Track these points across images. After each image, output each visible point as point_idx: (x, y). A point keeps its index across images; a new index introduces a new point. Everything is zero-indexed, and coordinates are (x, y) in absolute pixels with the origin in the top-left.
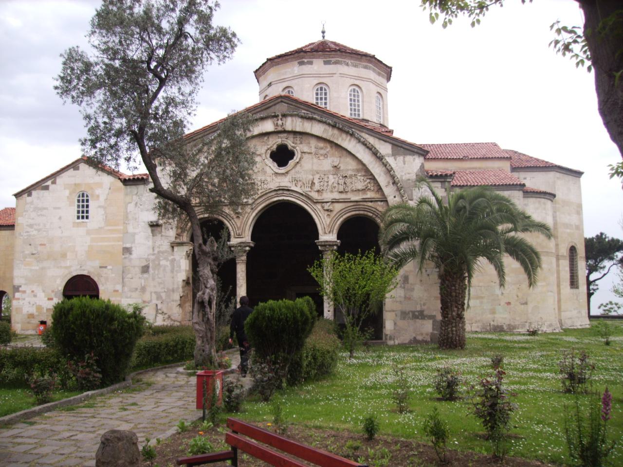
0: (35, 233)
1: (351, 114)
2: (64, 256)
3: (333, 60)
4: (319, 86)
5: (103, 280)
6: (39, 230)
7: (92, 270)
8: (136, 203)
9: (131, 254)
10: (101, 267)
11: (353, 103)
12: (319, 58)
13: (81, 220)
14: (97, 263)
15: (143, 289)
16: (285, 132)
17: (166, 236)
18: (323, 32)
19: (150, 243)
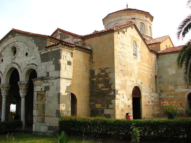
0: (121, 57)
6: (123, 56)
18: (127, 6)
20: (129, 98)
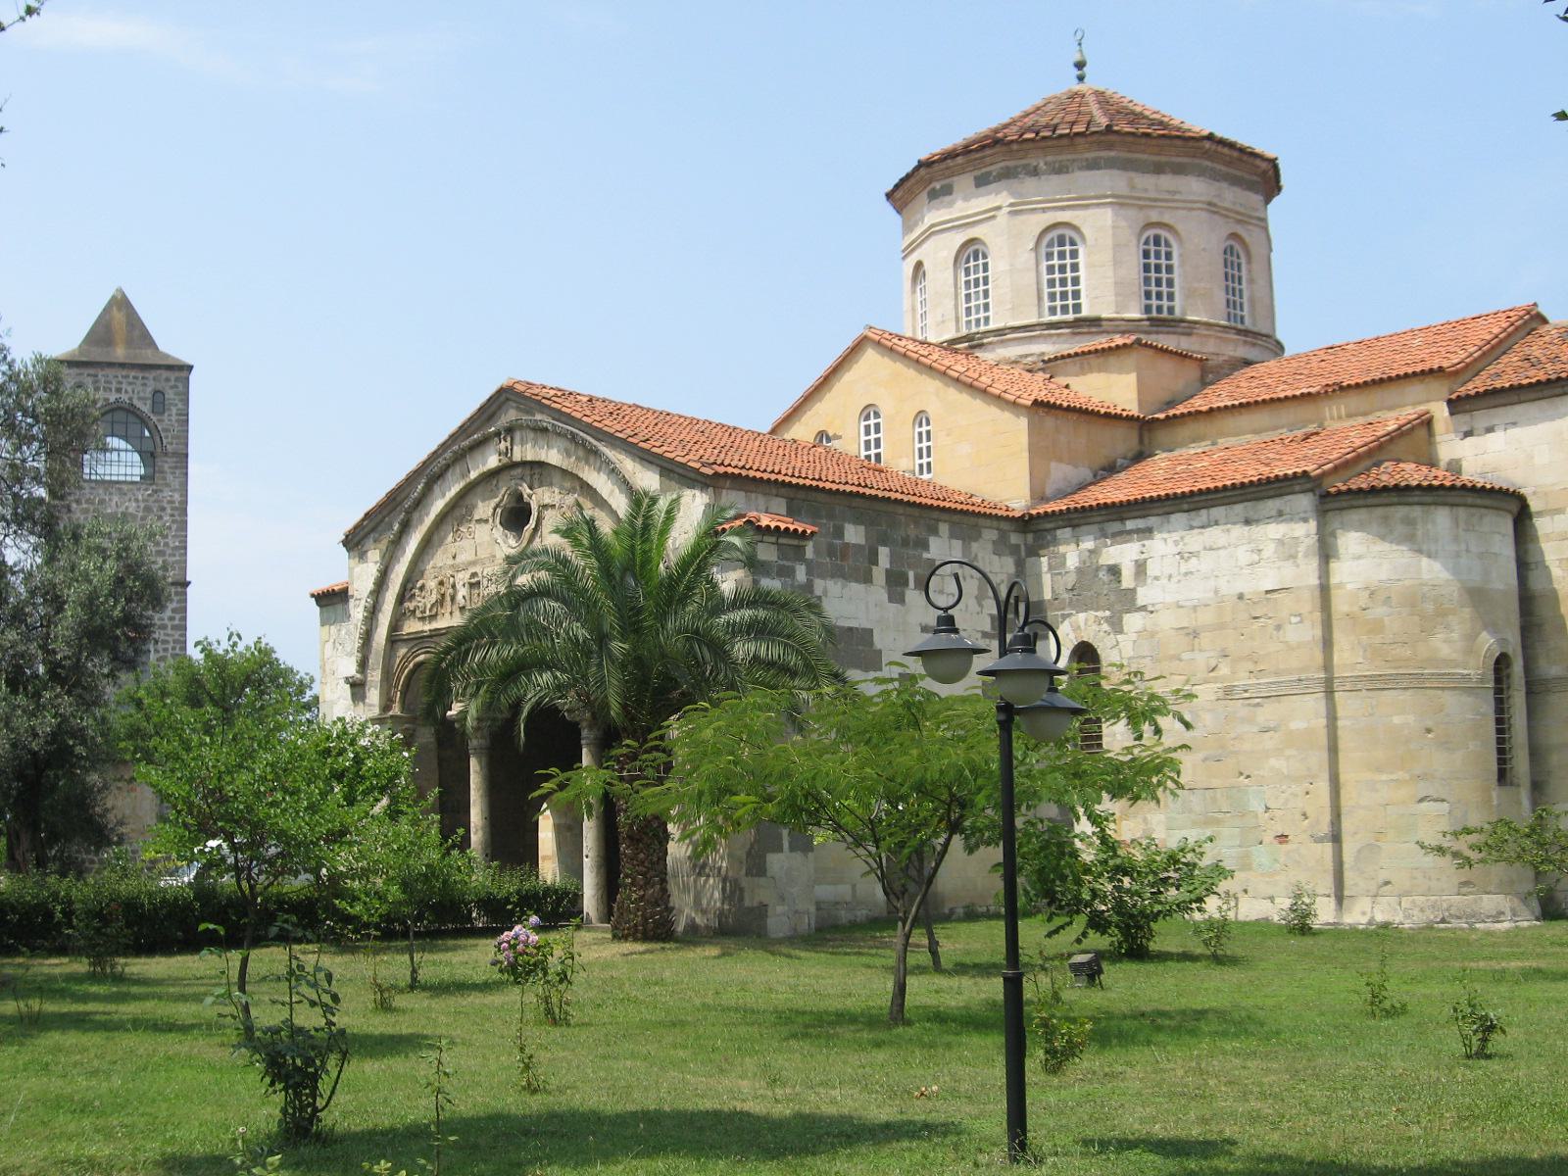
1: (1053, 311)
3: (995, 169)
11: (1057, 276)
16: (514, 465)
18: (1080, 65)
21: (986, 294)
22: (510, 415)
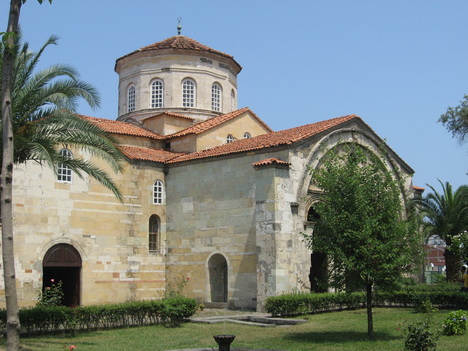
2: (45, 220)
3: (225, 64)
4: (215, 84)
5: (86, 249)
7: (76, 239)
8: (282, 185)
9: (280, 229)
10: (84, 236)
12: (216, 59)
13: (62, 181)
14: (80, 231)
15: (289, 261)
16: (357, 144)
17: (300, 216)
19: (292, 221)
20: (31, 267)
21: (218, 101)
22: (355, 127)
